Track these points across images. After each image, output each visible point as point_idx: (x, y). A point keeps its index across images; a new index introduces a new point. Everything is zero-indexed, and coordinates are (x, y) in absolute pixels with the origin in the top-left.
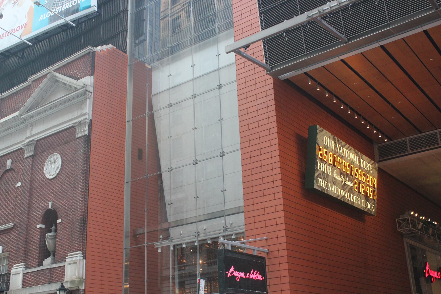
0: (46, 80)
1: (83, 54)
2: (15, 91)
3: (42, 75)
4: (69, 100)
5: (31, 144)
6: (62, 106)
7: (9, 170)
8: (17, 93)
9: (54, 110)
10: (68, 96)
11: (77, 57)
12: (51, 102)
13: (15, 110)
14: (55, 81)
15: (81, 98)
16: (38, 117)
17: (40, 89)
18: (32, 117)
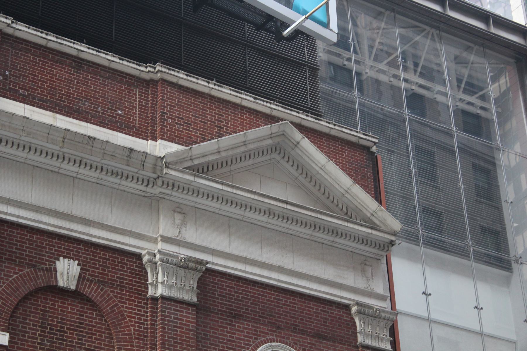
0: (264, 130)
1: (353, 139)
2: (74, 53)
3: (206, 91)
4: (316, 226)
5: (196, 269)
6: (306, 232)
7: (64, 292)
8: (79, 62)
9: (274, 221)
10: (319, 216)
11: (333, 133)
12: (255, 193)
13: (77, 111)
14: (280, 149)
15: (367, 248)
16: (214, 205)
17: (243, 140)
18: (197, 192)
